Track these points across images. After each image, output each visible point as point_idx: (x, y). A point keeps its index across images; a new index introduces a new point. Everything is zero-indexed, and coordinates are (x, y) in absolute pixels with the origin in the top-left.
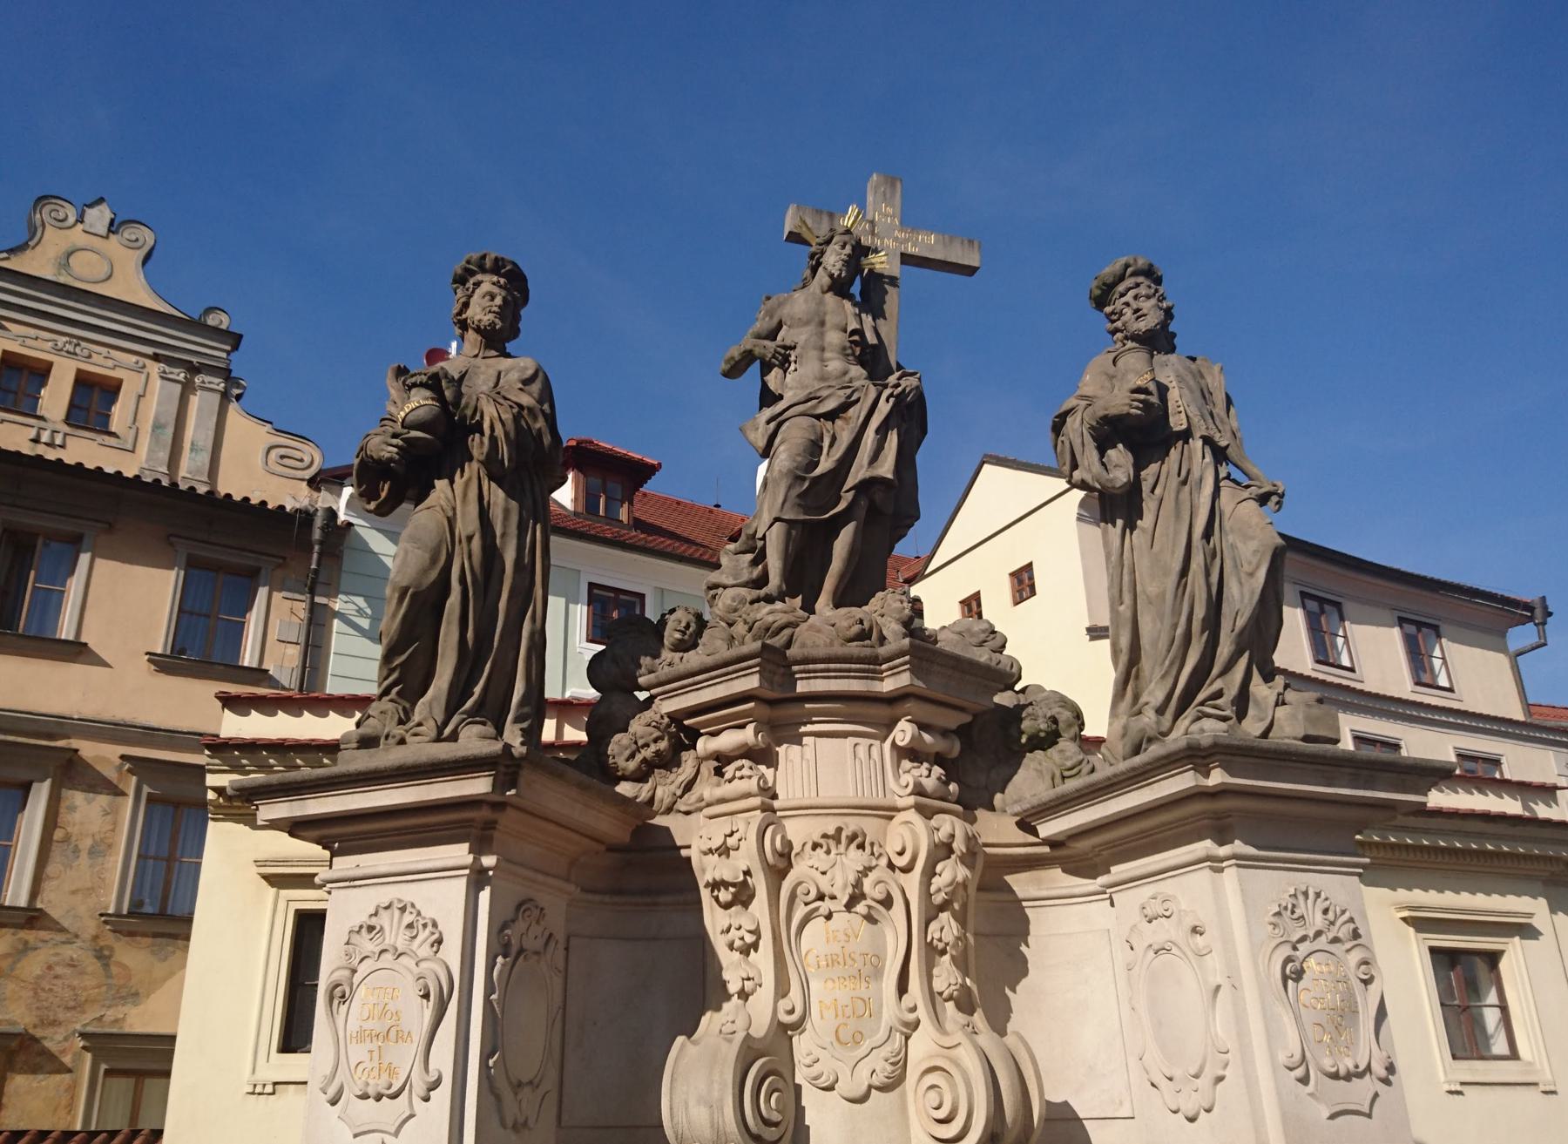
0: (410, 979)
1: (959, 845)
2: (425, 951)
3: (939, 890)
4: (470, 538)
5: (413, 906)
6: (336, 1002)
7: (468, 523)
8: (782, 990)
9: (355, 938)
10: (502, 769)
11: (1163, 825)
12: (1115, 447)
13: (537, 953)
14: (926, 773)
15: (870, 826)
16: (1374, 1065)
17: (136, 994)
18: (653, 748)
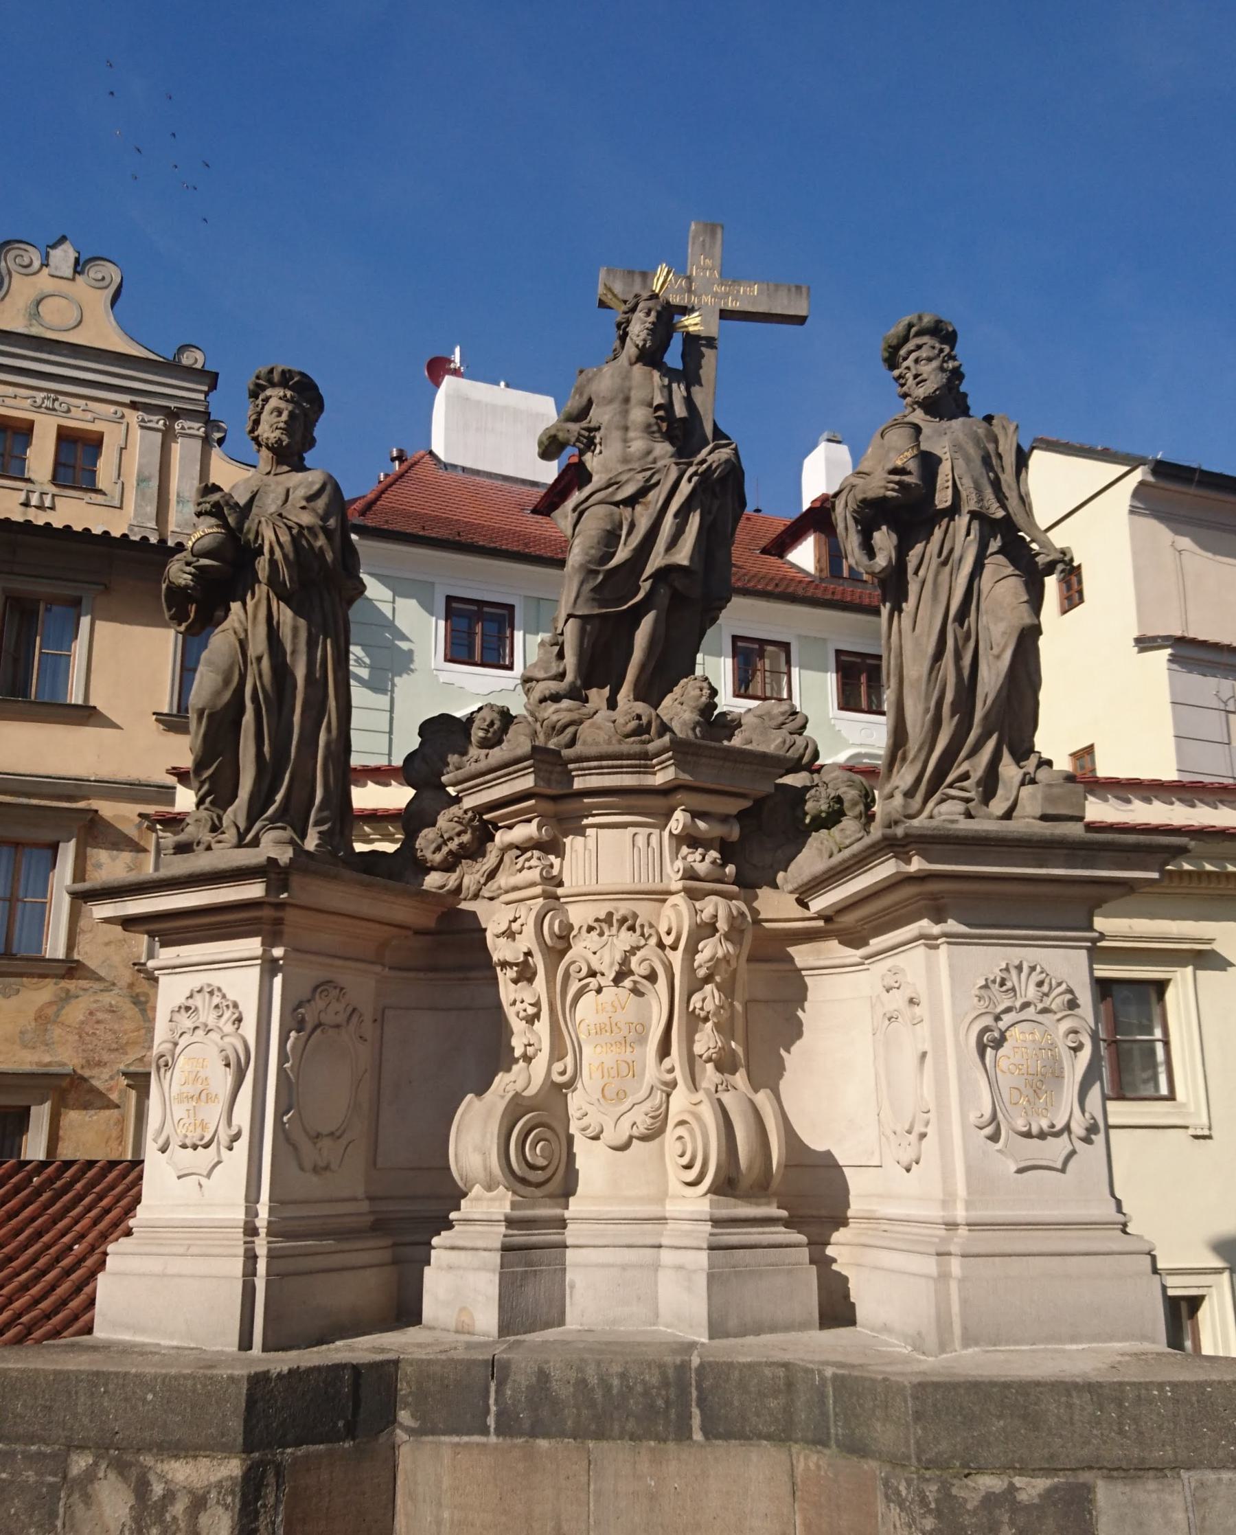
0: (216, 1050)
1: (722, 925)
2: (229, 1028)
3: (700, 966)
4: (259, 659)
5: (219, 989)
6: (162, 1070)
7: (258, 644)
8: (557, 1052)
9: (177, 1017)
10: (273, 876)
11: (897, 904)
12: (879, 529)
13: (338, 1026)
14: (699, 858)
15: (644, 910)
16: (1074, 1126)
18: (457, 841)
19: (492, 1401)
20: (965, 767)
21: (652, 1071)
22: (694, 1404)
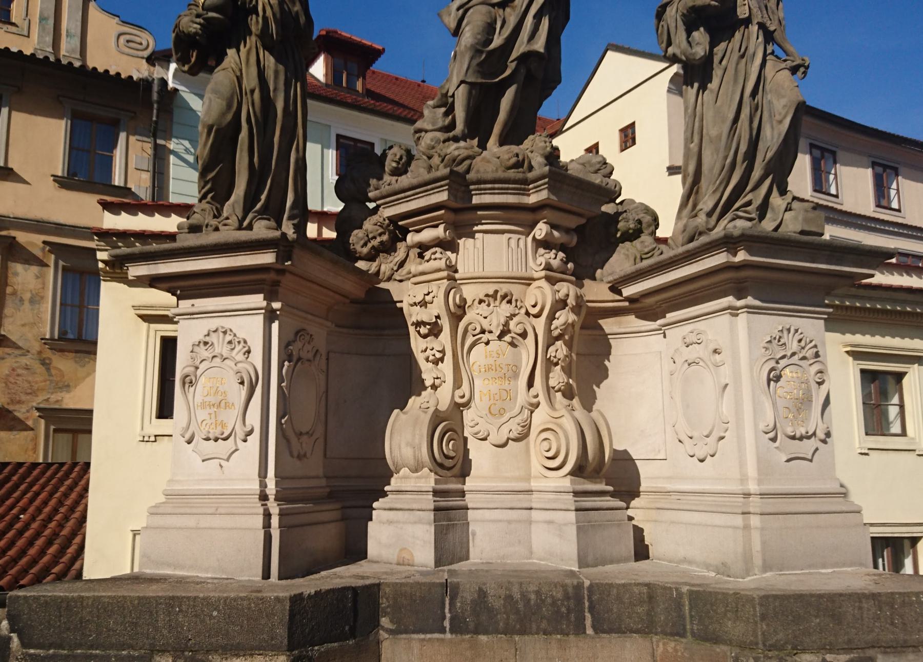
0: (232, 373)
1: (571, 301)
2: (240, 357)
3: (557, 328)
4: (252, 91)
5: (231, 330)
6: (187, 386)
7: (251, 80)
8: (457, 384)
9: (196, 349)
10: (281, 248)
11: (703, 287)
12: (698, 29)
13: (309, 360)
14: (553, 256)
15: (516, 290)
16: (818, 432)
17: (68, 386)
18: (379, 239)
19: (447, 610)
21: (522, 396)
22: (586, 610)
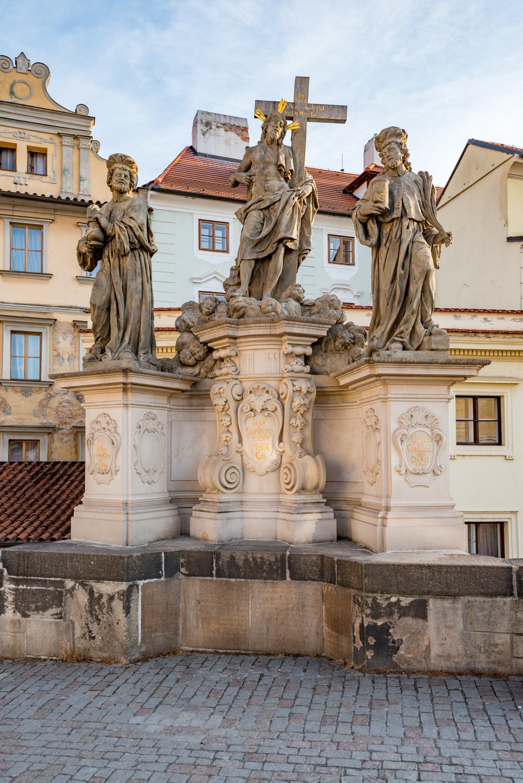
19: (214, 566)
20: (402, 328)
